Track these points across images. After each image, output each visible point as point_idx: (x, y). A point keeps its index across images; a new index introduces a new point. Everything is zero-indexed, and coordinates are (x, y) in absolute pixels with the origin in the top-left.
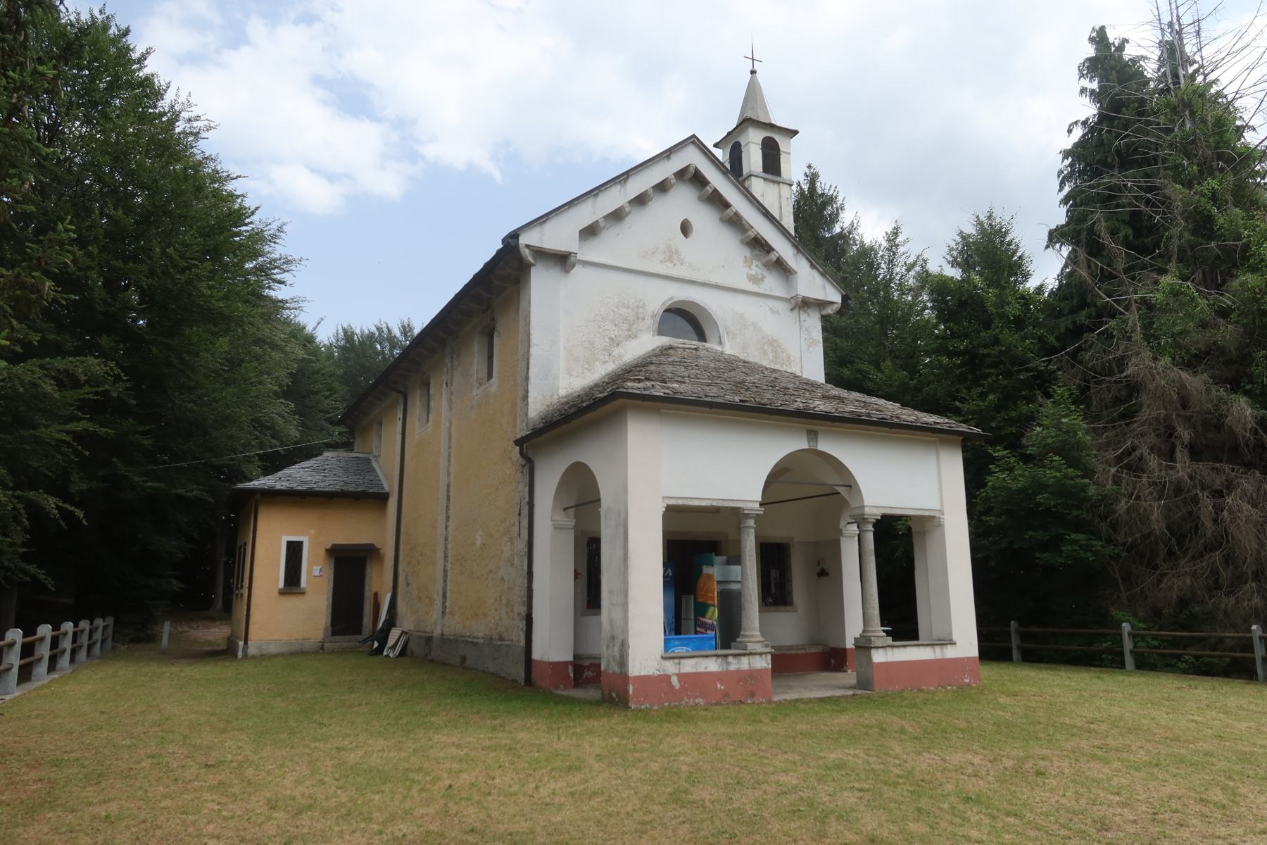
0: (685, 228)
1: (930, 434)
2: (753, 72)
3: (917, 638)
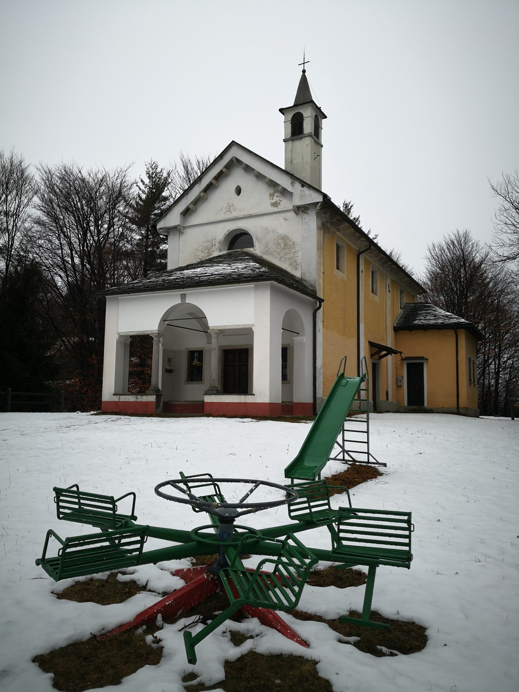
0: (238, 191)
1: (182, 290)
2: (304, 71)
3: (247, 393)
